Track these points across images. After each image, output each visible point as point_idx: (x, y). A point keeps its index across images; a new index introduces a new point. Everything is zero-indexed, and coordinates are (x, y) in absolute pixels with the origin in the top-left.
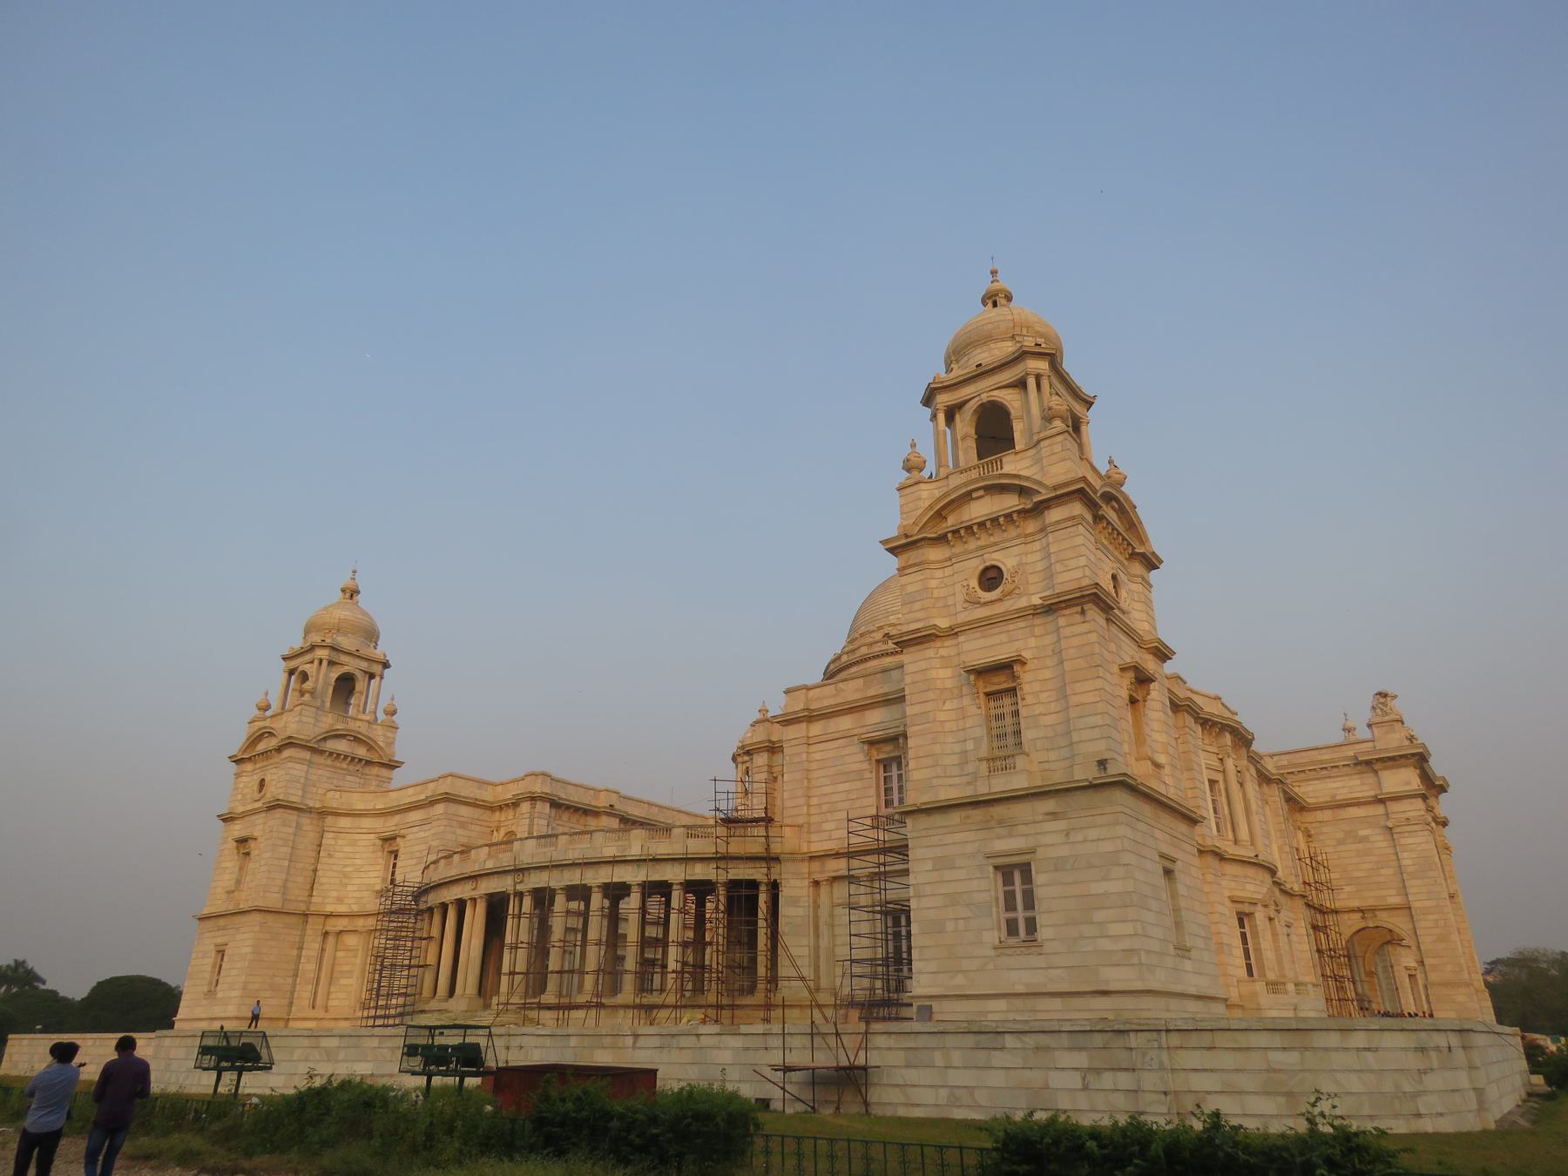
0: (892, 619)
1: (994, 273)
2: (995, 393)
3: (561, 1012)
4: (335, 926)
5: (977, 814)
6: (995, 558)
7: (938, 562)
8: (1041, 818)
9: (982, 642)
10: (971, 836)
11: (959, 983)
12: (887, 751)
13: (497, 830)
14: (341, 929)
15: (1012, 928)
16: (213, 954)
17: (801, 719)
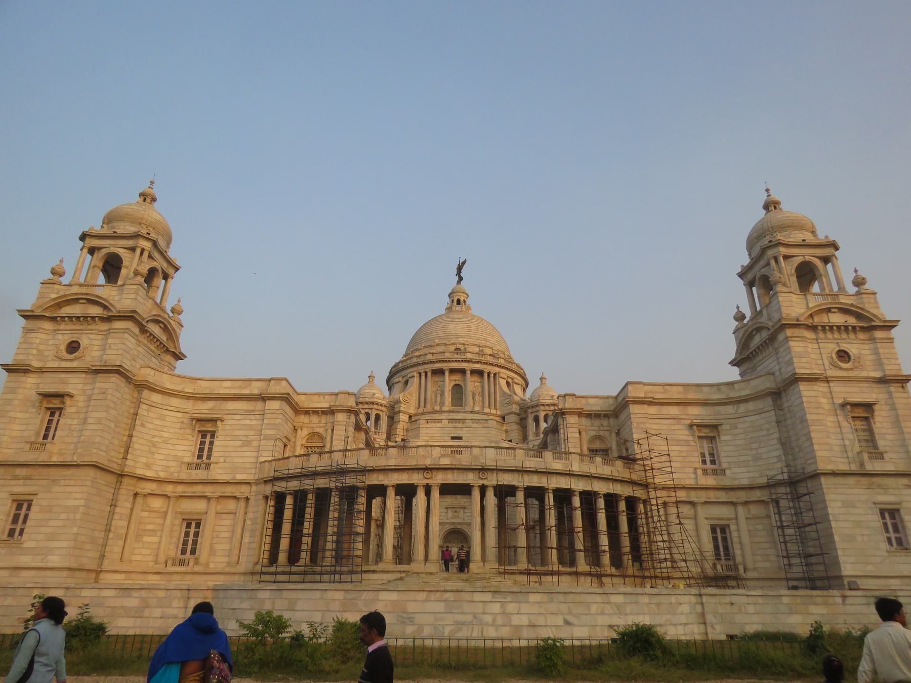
0: (461, 340)
1: (767, 190)
2: (812, 258)
3: (539, 576)
4: (144, 489)
5: (865, 480)
6: (845, 346)
7: (810, 339)
8: (901, 487)
9: (843, 389)
10: (862, 491)
11: (870, 569)
12: (705, 432)
13: (301, 430)
14: (149, 491)
15: (899, 541)
16: (9, 502)
17: (646, 402)
